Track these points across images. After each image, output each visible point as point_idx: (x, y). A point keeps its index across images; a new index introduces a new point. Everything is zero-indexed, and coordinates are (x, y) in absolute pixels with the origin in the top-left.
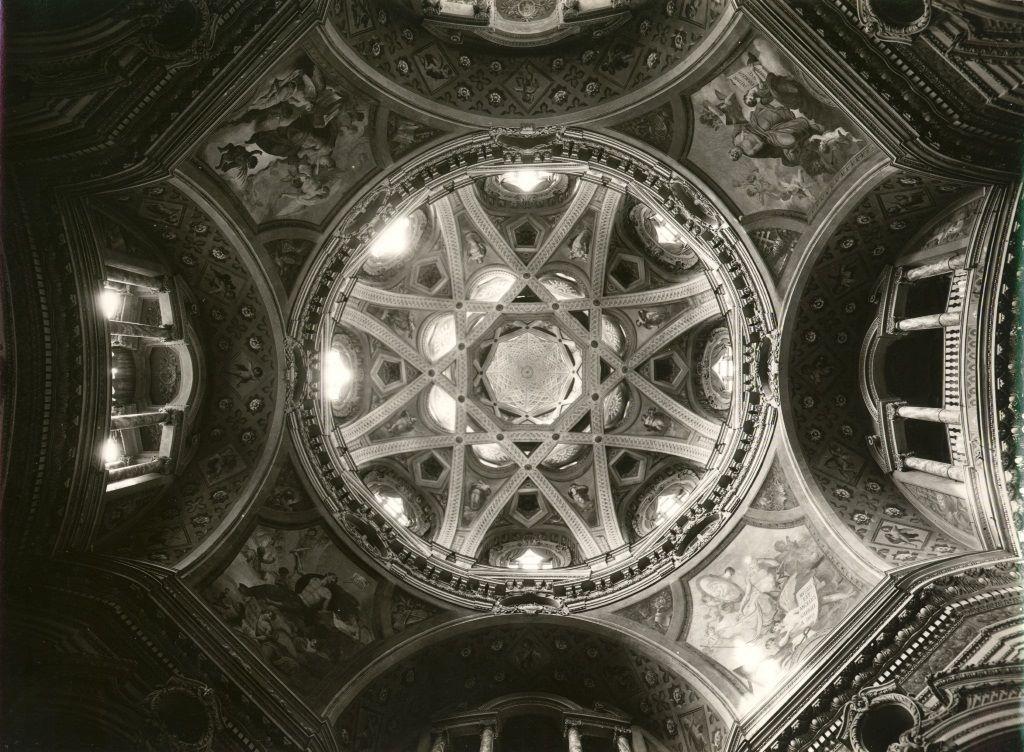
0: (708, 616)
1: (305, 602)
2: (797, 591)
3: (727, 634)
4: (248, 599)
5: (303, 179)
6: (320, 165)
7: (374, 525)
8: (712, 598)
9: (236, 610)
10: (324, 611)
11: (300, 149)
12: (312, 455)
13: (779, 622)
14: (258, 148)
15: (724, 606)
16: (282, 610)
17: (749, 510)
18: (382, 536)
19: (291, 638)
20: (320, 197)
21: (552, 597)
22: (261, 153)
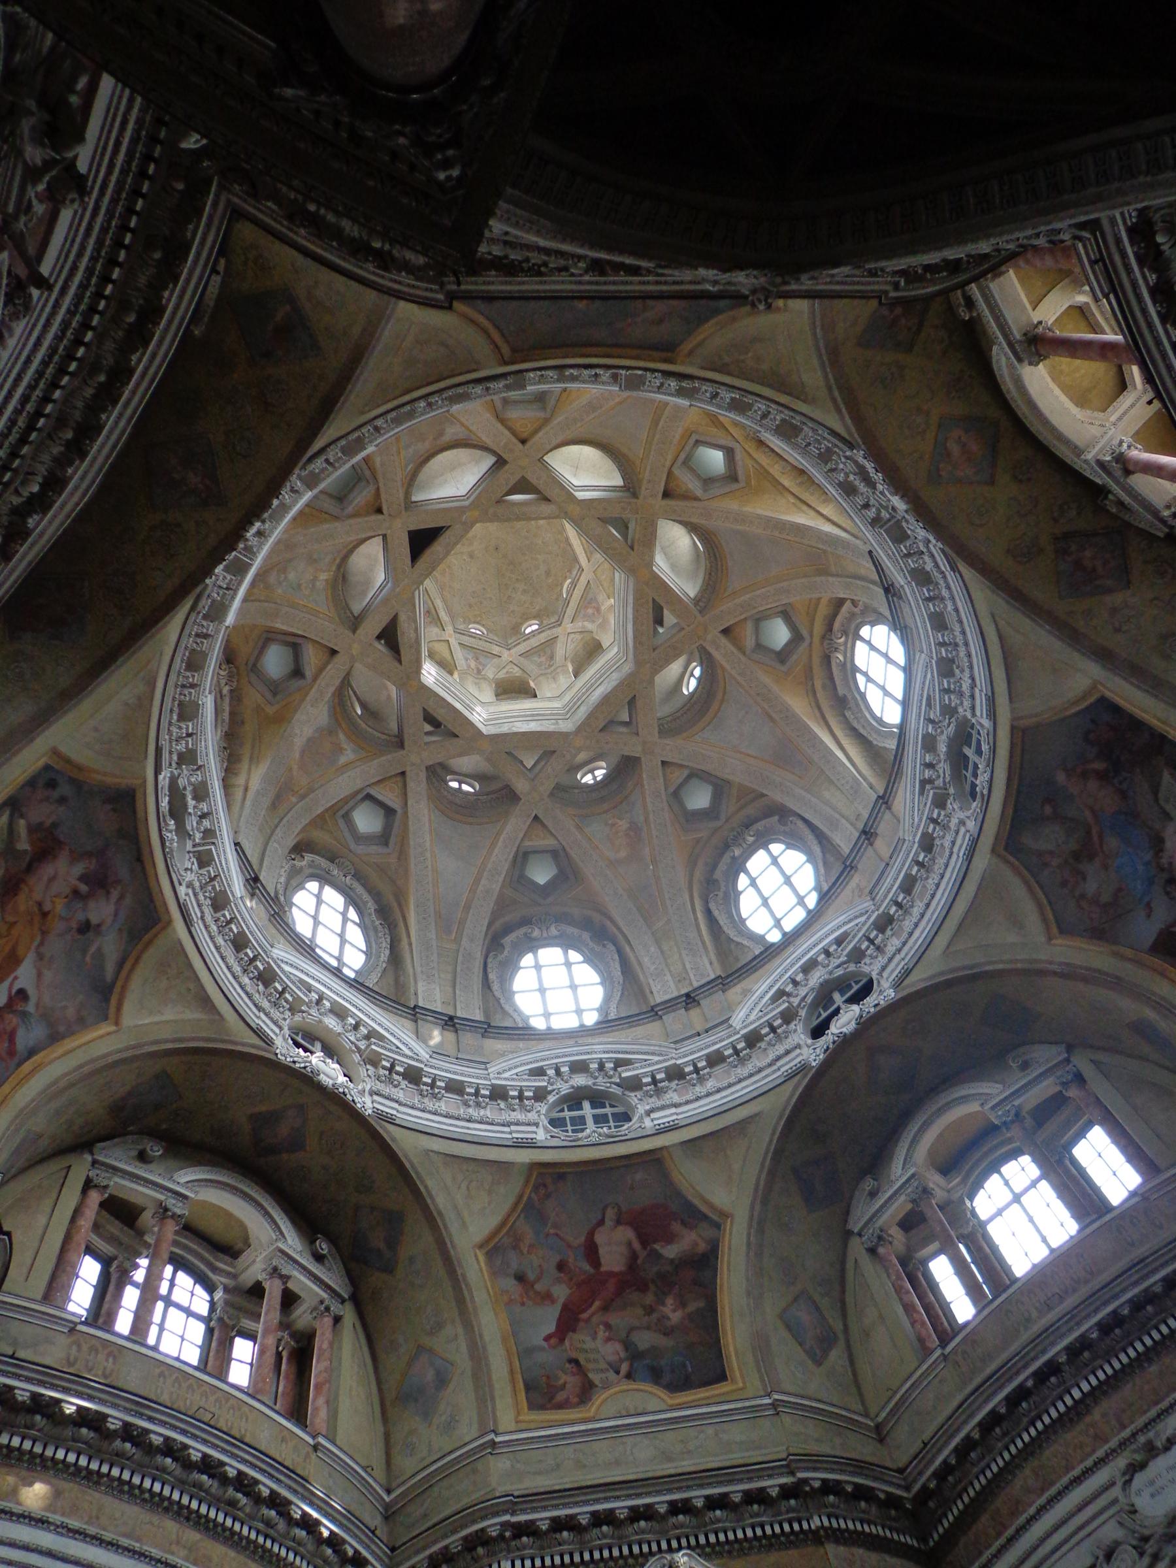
0: (1064, 884)
1: (616, 1269)
2: (1156, 800)
3: (1106, 898)
4: (567, 1342)
5: (80, 916)
6: (83, 878)
7: (580, 1080)
8: (1051, 853)
9: (574, 1374)
10: (642, 1254)
11: (40, 904)
12: (442, 1106)
13: (1161, 850)
14: (10, 979)
15: (1077, 856)
16: (605, 1308)
17: (1012, 711)
18: (602, 1083)
19: (648, 1328)
20: (122, 897)
21: (852, 967)
22: (16, 978)
